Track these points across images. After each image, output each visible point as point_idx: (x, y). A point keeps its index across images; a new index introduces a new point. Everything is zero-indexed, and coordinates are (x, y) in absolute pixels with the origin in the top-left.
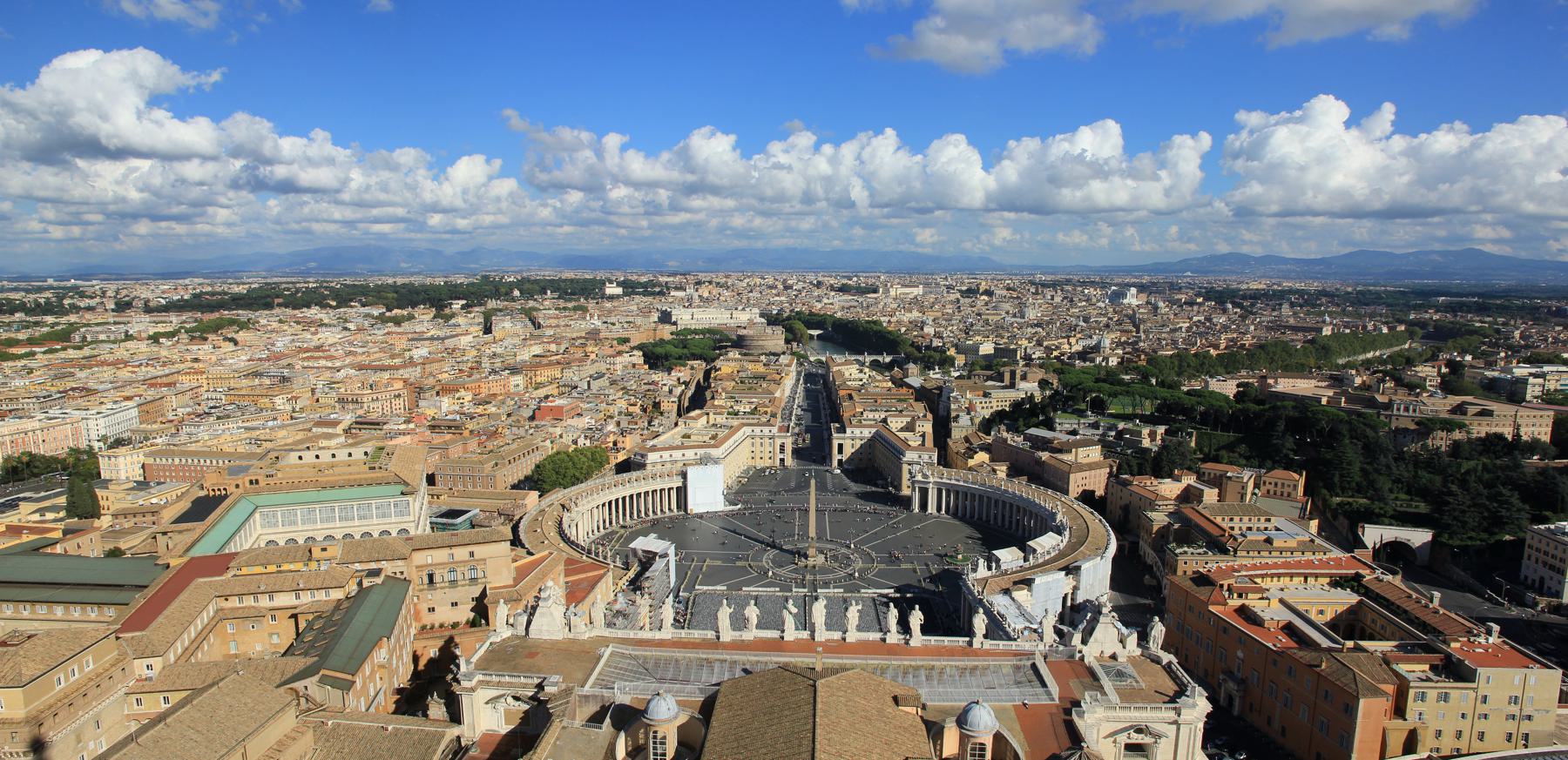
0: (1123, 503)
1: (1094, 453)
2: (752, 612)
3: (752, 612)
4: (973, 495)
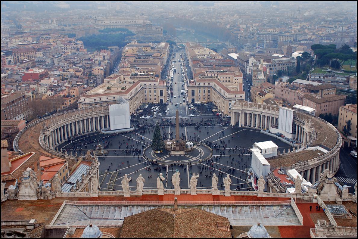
0: (347, 119)
1: (332, 93)
2: (140, 181)
3: (140, 181)
4: (264, 116)
